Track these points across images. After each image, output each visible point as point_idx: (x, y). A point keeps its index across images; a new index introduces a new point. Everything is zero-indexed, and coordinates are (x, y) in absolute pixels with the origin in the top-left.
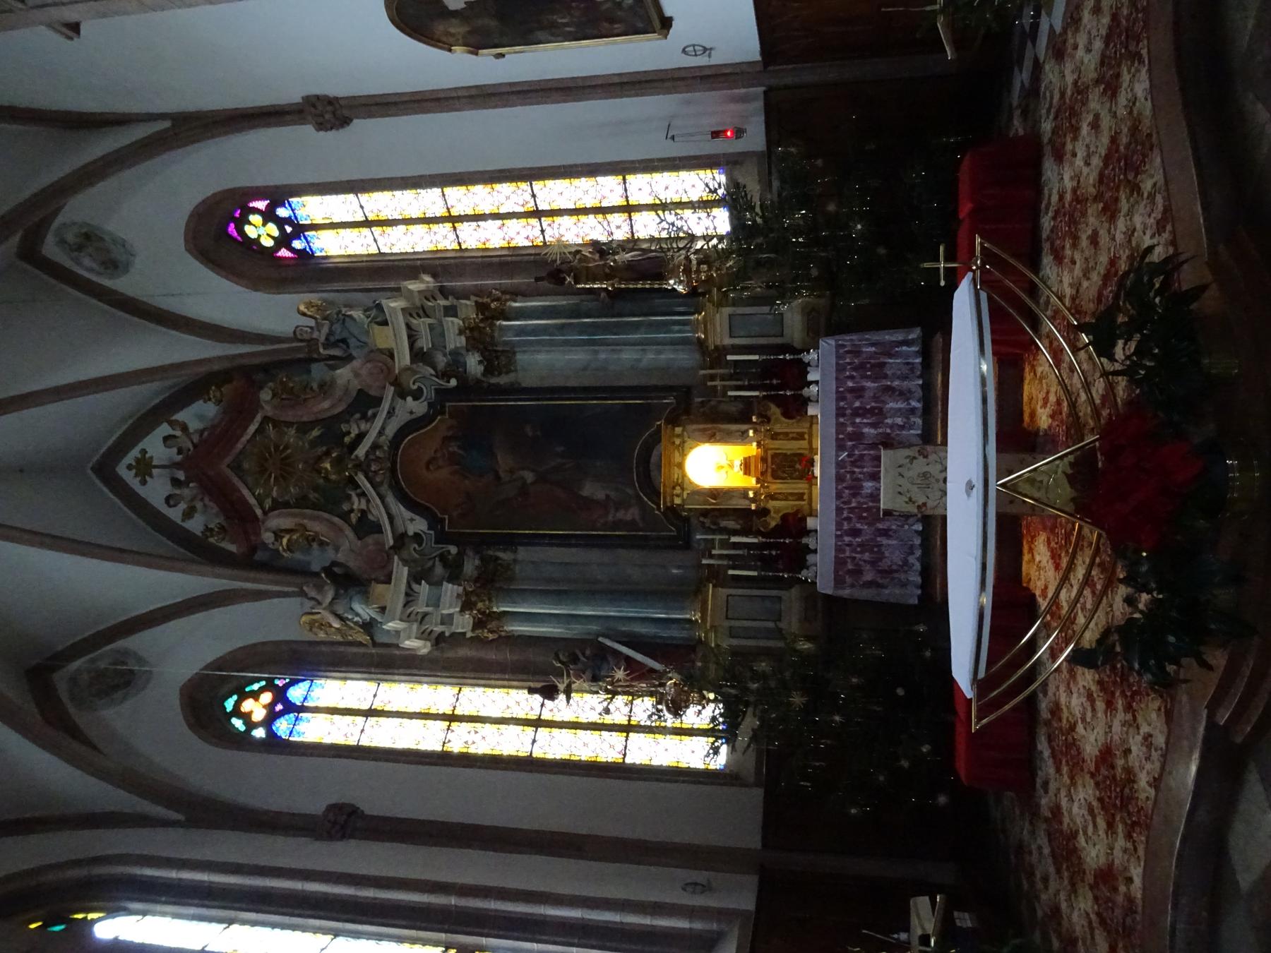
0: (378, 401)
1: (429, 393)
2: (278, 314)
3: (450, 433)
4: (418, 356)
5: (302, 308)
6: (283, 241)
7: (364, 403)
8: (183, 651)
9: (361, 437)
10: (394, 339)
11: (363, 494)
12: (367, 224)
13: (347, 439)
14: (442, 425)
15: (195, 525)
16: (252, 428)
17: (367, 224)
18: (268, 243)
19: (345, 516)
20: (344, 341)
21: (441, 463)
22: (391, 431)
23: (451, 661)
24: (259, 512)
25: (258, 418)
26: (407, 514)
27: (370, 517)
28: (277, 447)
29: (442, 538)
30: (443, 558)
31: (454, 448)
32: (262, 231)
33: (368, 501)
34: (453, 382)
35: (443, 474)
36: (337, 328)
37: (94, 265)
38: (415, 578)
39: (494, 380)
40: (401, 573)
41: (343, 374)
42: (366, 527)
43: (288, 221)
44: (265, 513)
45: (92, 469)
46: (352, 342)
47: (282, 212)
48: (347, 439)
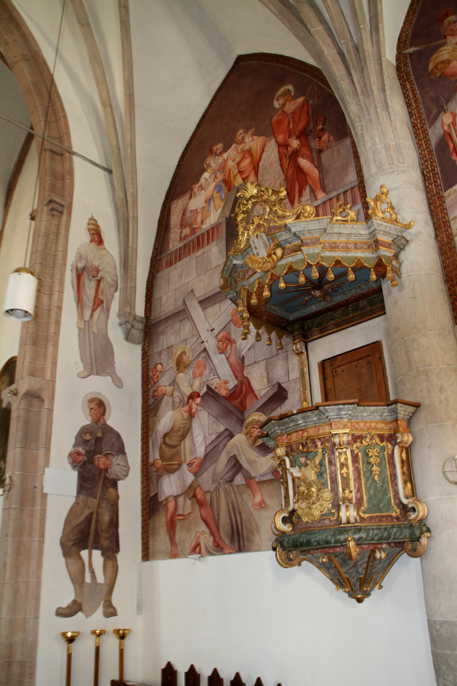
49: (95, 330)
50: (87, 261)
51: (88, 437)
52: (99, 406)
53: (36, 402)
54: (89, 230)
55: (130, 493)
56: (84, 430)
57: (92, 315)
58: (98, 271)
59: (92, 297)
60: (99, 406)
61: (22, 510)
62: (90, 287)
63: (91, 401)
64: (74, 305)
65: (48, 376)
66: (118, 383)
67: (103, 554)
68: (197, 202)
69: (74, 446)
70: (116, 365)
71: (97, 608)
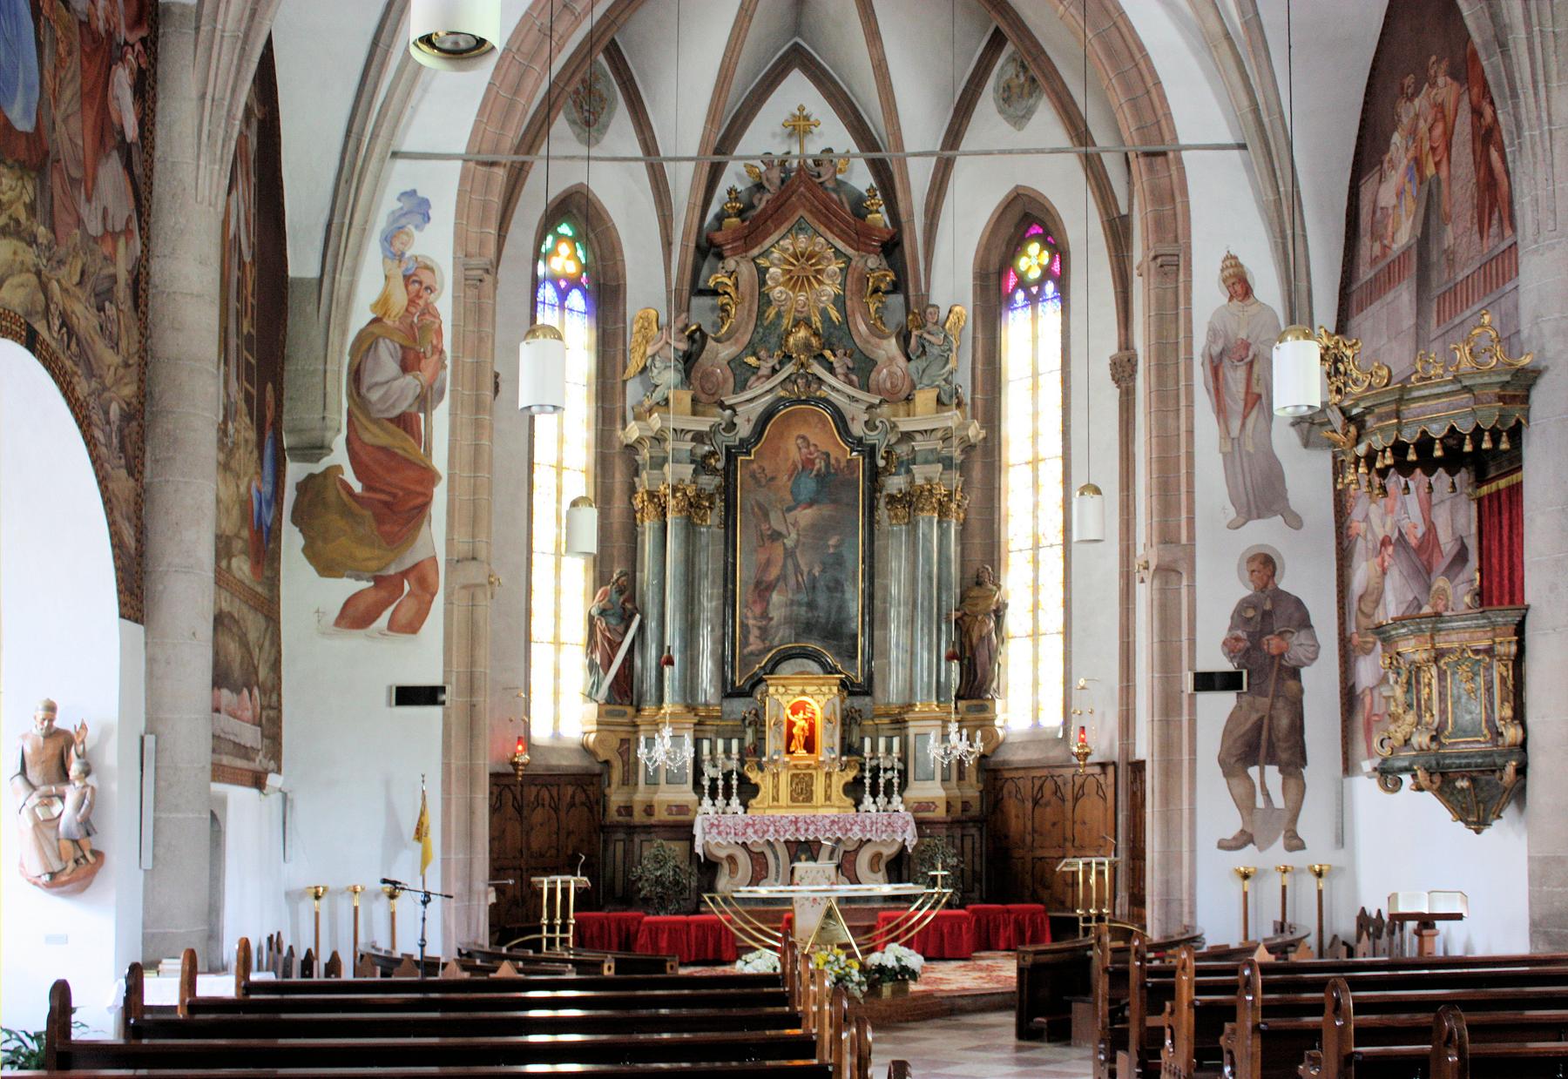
0: (865, 387)
1: (873, 437)
2: (950, 280)
3: (833, 461)
4: (908, 436)
5: (957, 309)
6: (1022, 283)
7: (862, 369)
8: (621, 191)
9: (831, 369)
10: (923, 415)
11: (774, 371)
12: (1035, 375)
13: (828, 353)
14: (843, 453)
15: (734, 177)
16: (840, 245)
17: (1035, 375)
18: (1023, 263)
19: (752, 349)
20: (924, 352)
21: (804, 450)
22: (835, 397)
23: (616, 462)
24: (755, 252)
25: (850, 251)
26: (754, 417)
27: (753, 378)
28: (818, 271)
29: (731, 456)
30: (713, 454)
31: (819, 464)
32: (1034, 262)
33: (768, 378)
34: (881, 463)
35: (792, 451)
36: (936, 351)
37: (1006, 77)
38: (699, 437)
39: (882, 503)
40: (702, 424)
41: (891, 346)
42: (742, 374)
43: (1041, 291)
44: (753, 260)
45: (796, 43)
46: (922, 363)
47: (1050, 287)
48: (828, 353)
49: (1251, 449)
50: (1226, 337)
51: (1250, 613)
52: (1264, 565)
53: (1173, 576)
54: (1224, 281)
55: (1319, 686)
56: (1245, 604)
57: (1243, 425)
58: (1247, 346)
59: (1241, 388)
60: (1264, 565)
61: (1168, 722)
62: (1235, 379)
63: (1252, 559)
64: (1213, 417)
65: (1184, 540)
66: (1295, 521)
67: (1281, 771)
68: (1387, 196)
69: (1231, 629)
70: (1290, 495)
71: (1275, 839)
